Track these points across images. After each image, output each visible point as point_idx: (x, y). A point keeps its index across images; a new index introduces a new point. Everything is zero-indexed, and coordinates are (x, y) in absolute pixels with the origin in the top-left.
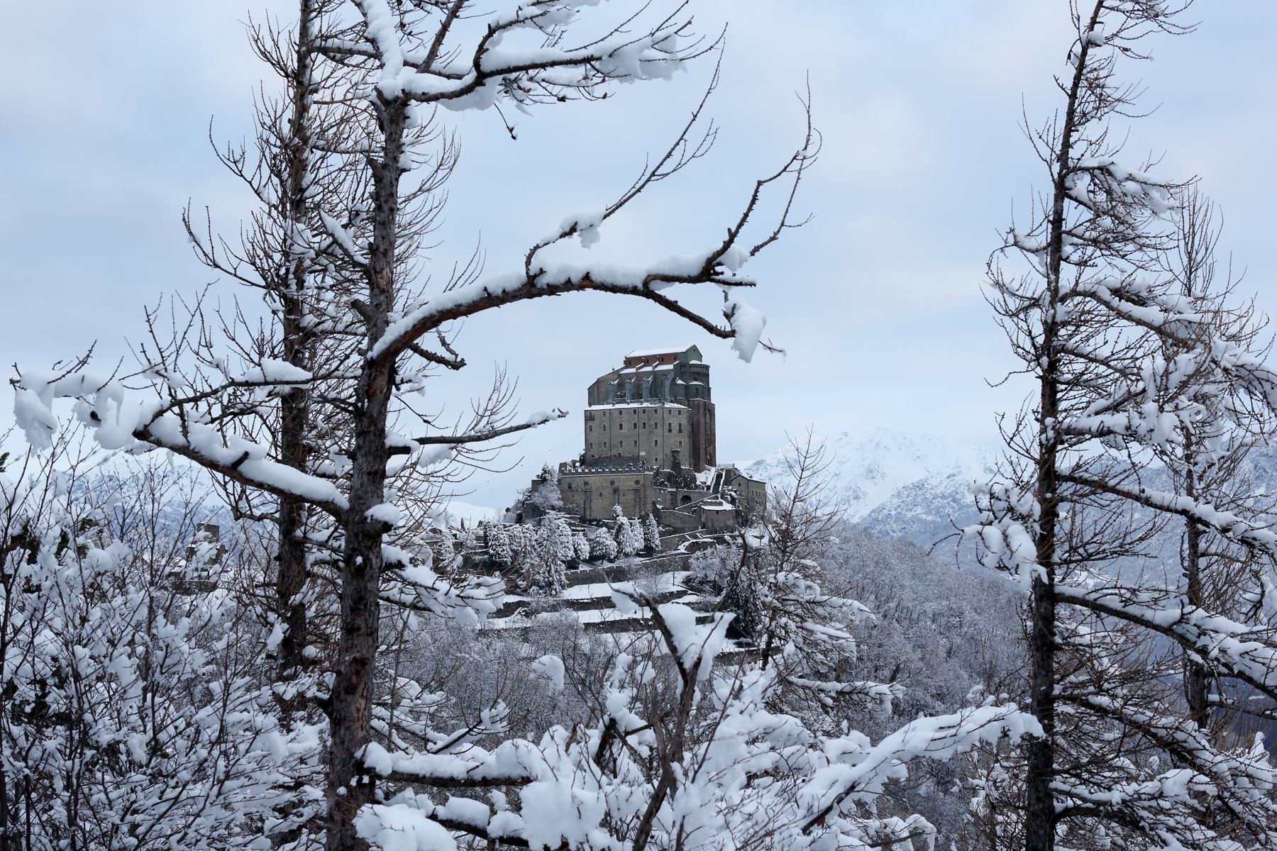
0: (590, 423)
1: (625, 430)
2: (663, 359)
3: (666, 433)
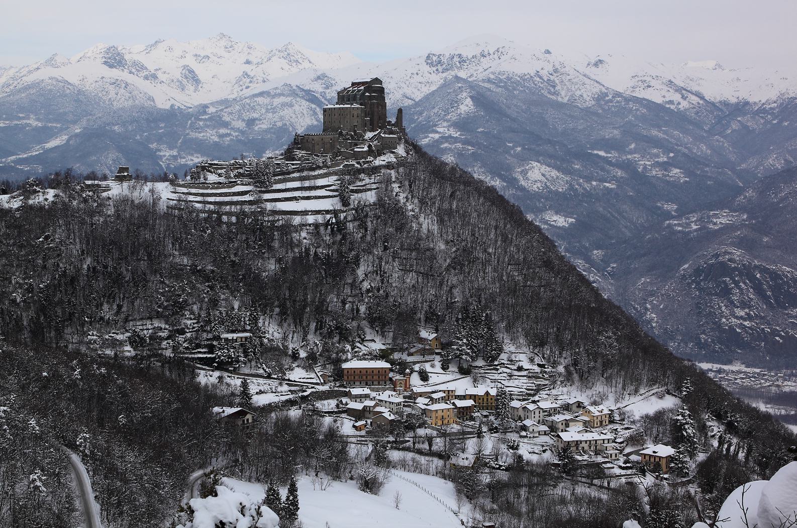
2: (363, 83)
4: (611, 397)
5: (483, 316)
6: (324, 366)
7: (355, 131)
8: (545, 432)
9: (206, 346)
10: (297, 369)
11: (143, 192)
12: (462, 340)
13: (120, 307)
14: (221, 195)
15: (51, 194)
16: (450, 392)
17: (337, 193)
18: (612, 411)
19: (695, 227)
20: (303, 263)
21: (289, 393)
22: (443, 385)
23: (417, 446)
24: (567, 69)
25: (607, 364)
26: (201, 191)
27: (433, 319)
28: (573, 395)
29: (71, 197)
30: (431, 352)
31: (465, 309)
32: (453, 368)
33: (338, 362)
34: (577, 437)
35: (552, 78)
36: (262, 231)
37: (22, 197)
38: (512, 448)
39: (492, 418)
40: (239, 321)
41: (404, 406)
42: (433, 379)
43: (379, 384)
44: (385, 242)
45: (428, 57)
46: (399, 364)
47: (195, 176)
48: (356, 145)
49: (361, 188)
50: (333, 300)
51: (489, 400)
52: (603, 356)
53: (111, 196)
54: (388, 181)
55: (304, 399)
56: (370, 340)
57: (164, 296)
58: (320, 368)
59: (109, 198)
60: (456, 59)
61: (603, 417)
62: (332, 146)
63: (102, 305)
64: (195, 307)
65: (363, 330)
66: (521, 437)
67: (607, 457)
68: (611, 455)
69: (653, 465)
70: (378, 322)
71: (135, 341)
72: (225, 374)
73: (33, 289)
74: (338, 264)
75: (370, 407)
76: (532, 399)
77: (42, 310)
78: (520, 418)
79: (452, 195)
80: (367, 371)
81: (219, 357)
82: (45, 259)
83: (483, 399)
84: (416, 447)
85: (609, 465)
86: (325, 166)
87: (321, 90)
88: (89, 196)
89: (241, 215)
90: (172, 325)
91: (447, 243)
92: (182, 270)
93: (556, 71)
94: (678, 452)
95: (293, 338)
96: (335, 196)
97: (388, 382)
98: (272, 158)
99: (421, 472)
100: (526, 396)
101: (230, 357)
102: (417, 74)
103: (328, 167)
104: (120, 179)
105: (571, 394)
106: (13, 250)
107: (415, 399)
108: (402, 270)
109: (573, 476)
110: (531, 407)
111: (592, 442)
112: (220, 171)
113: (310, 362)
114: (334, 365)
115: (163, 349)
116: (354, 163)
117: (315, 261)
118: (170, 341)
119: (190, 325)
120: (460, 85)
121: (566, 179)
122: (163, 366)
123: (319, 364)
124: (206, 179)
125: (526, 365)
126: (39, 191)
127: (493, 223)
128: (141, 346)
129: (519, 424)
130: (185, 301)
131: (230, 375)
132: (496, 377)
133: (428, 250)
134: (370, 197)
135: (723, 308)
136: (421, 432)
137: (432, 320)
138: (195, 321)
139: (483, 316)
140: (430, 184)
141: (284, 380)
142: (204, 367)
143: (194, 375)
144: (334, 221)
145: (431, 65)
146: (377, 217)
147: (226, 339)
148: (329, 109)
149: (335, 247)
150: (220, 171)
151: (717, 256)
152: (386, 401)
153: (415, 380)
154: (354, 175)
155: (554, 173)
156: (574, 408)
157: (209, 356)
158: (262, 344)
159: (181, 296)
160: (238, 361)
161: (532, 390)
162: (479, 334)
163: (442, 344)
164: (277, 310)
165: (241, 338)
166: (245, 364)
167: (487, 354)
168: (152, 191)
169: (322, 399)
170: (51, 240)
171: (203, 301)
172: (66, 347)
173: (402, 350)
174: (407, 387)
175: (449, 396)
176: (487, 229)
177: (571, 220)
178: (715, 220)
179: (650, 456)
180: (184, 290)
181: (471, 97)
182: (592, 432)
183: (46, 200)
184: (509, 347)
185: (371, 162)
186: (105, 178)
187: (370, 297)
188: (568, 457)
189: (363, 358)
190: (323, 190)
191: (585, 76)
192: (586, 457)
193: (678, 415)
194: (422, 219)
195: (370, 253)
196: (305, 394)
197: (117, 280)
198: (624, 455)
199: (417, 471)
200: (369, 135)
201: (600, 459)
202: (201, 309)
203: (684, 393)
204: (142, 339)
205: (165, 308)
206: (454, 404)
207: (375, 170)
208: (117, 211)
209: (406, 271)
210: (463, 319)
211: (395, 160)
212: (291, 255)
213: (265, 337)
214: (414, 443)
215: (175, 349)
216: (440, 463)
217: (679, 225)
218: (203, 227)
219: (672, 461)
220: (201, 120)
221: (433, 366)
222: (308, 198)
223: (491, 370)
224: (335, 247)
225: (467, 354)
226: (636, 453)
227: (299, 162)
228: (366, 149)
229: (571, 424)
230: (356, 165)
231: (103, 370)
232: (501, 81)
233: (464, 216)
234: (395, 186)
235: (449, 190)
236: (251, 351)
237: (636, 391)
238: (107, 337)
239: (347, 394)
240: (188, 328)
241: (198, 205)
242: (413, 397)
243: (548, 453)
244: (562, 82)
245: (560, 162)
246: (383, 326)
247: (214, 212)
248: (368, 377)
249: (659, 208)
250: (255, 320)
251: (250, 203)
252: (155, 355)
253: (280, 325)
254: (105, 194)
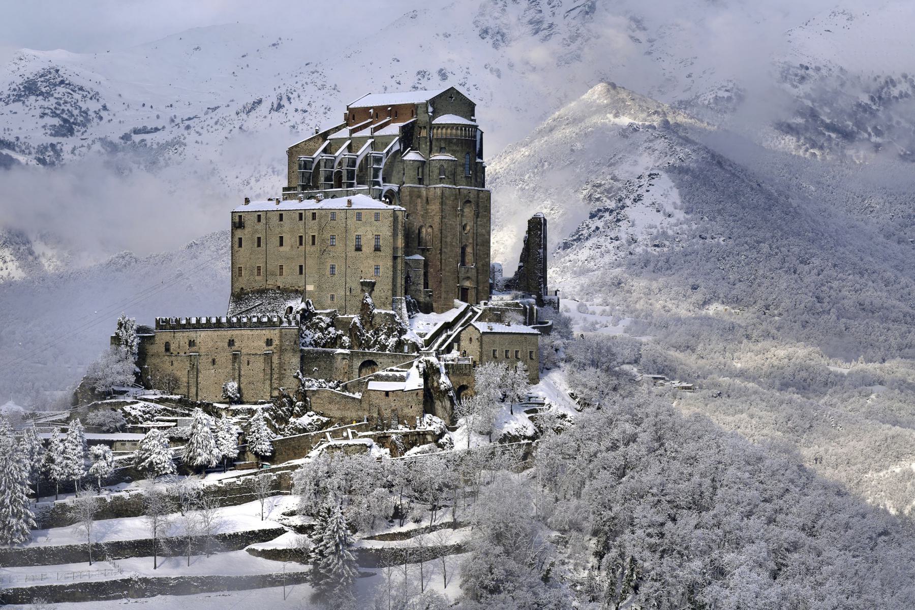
0: (239, 233)
1: (285, 248)
2: (394, 112)
3: (352, 253)
96: (296, 579)
116: (368, 441)
190: (243, 553)
200: (422, 326)
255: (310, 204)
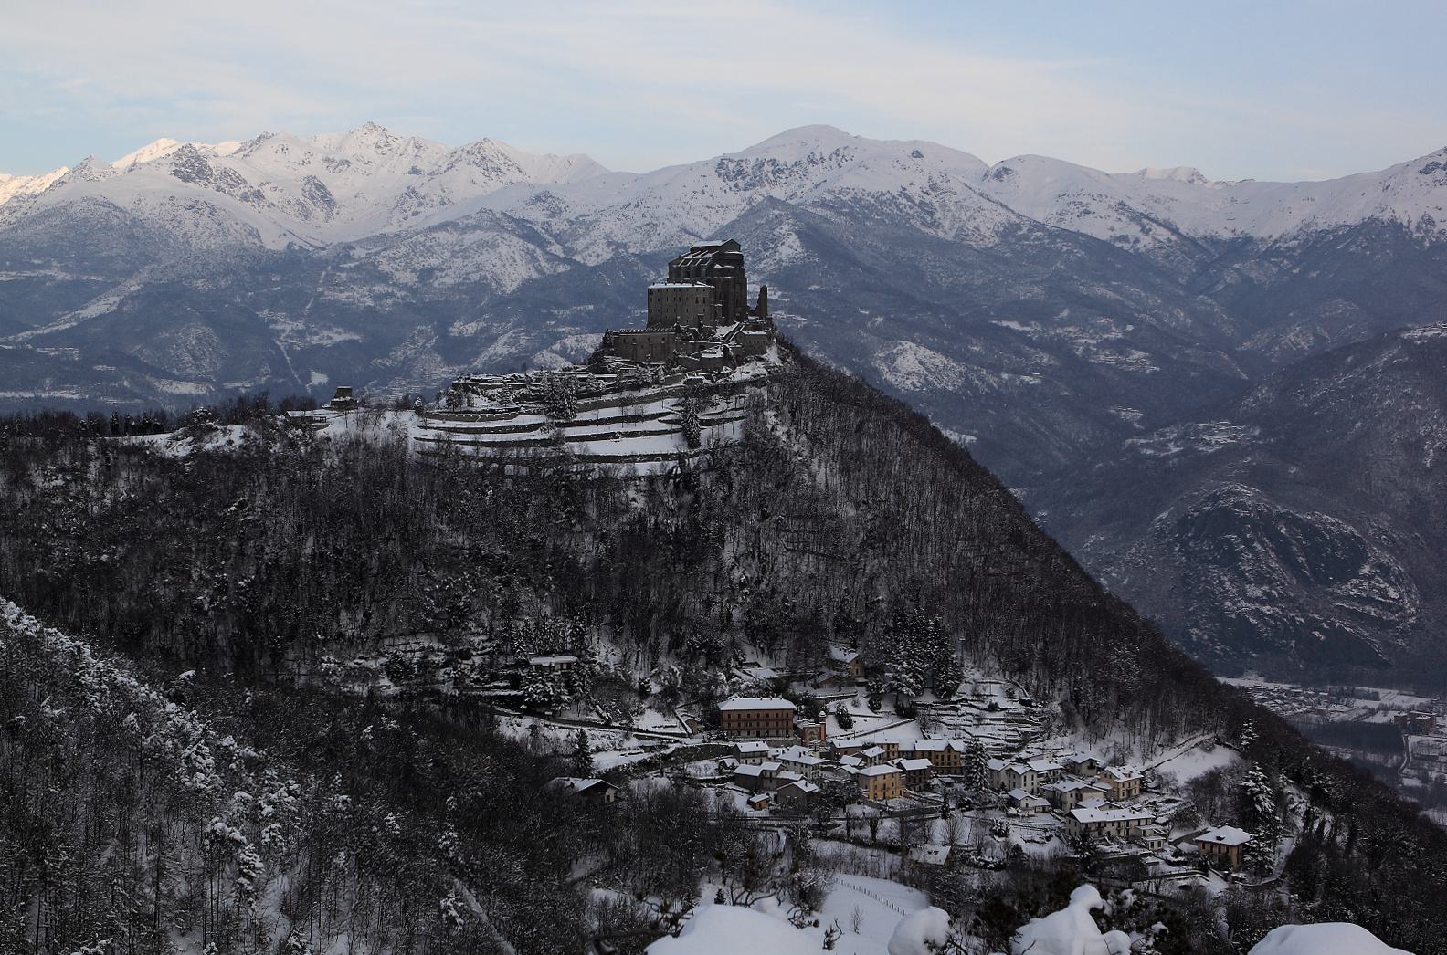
1: (669, 302)
2: (711, 249)
4: (1137, 754)
5: (929, 625)
6: (688, 707)
7: (700, 326)
8: (1044, 807)
9: (506, 677)
10: (648, 712)
11: (380, 430)
12: (901, 664)
13: (367, 616)
14: (496, 430)
15: (237, 432)
16: (891, 747)
17: (679, 427)
18: (1142, 773)
19: (1175, 450)
20: (639, 540)
21: (641, 750)
22: (873, 732)
23: (853, 833)
24: (952, 185)
25: (1124, 699)
26: (465, 425)
27: (848, 629)
28: (1079, 750)
29: (269, 439)
30: (852, 683)
31: (899, 614)
32: (886, 707)
33: (709, 700)
34: (1100, 816)
35: (927, 199)
36: (568, 488)
37: (190, 439)
38: (999, 834)
39: (960, 787)
40: (557, 636)
41: (823, 769)
42: (859, 725)
43: (778, 735)
44: (761, 506)
45: (721, 165)
46: (805, 702)
47: (454, 402)
48: (702, 347)
49: (715, 417)
50: (692, 603)
51: (952, 757)
52: (1119, 686)
53: (331, 435)
54: (758, 407)
55: (666, 758)
56: (751, 664)
57: (433, 598)
58: (682, 709)
59: (328, 439)
60: (768, 168)
61: (1132, 784)
62: (665, 350)
63: (337, 613)
64: (484, 616)
65: (738, 646)
66: (1009, 816)
67: (1146, 847)
68: (1152, 843)
69: (1219, 859)
70: (764, 635)
71: (397, 671)
72: (542, 722)
73: (227, 588)
74: (694, 541)
75: (771, 772)
76: (1017, 755)
77: (248, 623)
78: (1003, 786)
79: (860, 426)
80: (758, 715)
81: (530, 695)
82: (243, 540)
83: (943, 757)
84: (852, 834)
85: (1150, 859)
86: (657, 382)
87: (542, 219)
88: (297, 436)
89: (536, 463)
90: (453, 644)
91: (857, 506)
92: (457, 555)
93: (934, 187)
94: (1256, 838)
95: (637, 662)
97: (791, 732)
98: (569, 369)
99: (866, 873)
100: (1006, 751)
101: (547, 694)
102: (703, 192)
103: (661, 384)
104: (342, 407)
105: (1072, 747)
106: (188, 525)
107: (839, 758)
108: (793, 550)
109: (1100, 877)
110: (1019, 769)
111: (1122, 824)
112: (490, 392)
113: (666, 702)
114: (705, 705)
115: (438, 682)
117: (656, 537)
118: (448, 670)
119: (479, 644)
120: (777, 212)
121: (963, 369)
122: (443, 711)
123: (682, 704)
124: (471, 405)
125: (1003, 703)
126: (217, 429)
127: (929, 474)
128: (406, 678)
129: (1003, 795)
130: (468, 606)
131: (548, 723)
132: (956, 720)
133: (831, 517)
134: (733, 432)
135: (1227, 585)
136: (857, 810)
137: (846, 630)
138: (484, 638)
139: (929, 625)
140: (823, 414)
141: (632, 730)
142: (506, 711)
143: (493, 724)
144: (679, 472)
145: (726, 177)
146: (744, 465)
147: (539, 667)
148: (658, 289)
149: (684, 512)
150: (490, 392)
151: (1214, 498)
152: (795, 763)
153: (832, 727)
154: (703, 396)
155: (940, 360)
156: (1084, 770)
157: (513, 693)
158: (593, 674)
159: (460, 597)
160: (560, 701)
161: (1015, 741)
162: (926, 654)
163: (866, 669)
164: (607, 618)
165: (562, 664)
166: (569, 705)
167: (939, 685)
168: (393, 427)
169: (690, 760)
170: (249, 510)
171: (495, 605)
172: (292, 681)
173: (803, 678)
174: (821, 734)
175: (888, 753)
176: (920, 484)
177: (969, 438)
178: (1207, 438)
179: (1212, 844)
180: (465, 588)
181: (798, 233)
182: (1120, 808)
183: (230, 442)
184: (971, 674)
185: (728, 375)
186: (311, 405)
187: (746, 594)
188: (1089, 849)
189: (746, 694)
191: (981, 195)
192: (1115, 848)
193: (1247, 780)
194: (814, 467)
195: (739, 523)
196: (668, 752)
197: (360, 574)
198: (1170, 843)
199: (860, 872)
200: (722, 331)
201: (1134, 850)
202: (493, 617)
203: (1244, 743)
204: (407, 668)
205: (436, 617)
206: (899, 765)
207: (737, 388)
208: (344, 460)
209: (799, 552)
210: (896, 629)
211: (764, 371)
212: (615, 526)
213: (595, 662)
214: (848, 829)
215: (458, 682)
216: (897, 859)
217: (1147, 446)
218: (480, 485)
219: (1247, 852)
220: (343, 270)
221: (855, 705)
222: (633, 434)
223: (946, 709)
224: (684, 512)
225: (910, 685)
226: (1188, 839)
227: (615, 376)
228: (720, 354)
229: (1085, 795)
230: (706, 381)
231: (393, 724)
232: (843, 204)
233: (882, 463)
234: (769, 413)
235: (853, 419)
236: (579, 686)
237: (1172, 740)
238: (352, 664)
239: (734, 752)
240: (476, 649)
241: (468, 449)
242: (833, 754)
243: (1055, 842)
244: (945, 205)
245: (946, 339)
246: (774, 639)
247: (492, 460)
248: (761, 724)
249: (1113, 417)
250: (579, 636)
251: (544, 443)
252: (426, 693)
253: (614, 641)
254: (321, 433)
255: (678, 285)
